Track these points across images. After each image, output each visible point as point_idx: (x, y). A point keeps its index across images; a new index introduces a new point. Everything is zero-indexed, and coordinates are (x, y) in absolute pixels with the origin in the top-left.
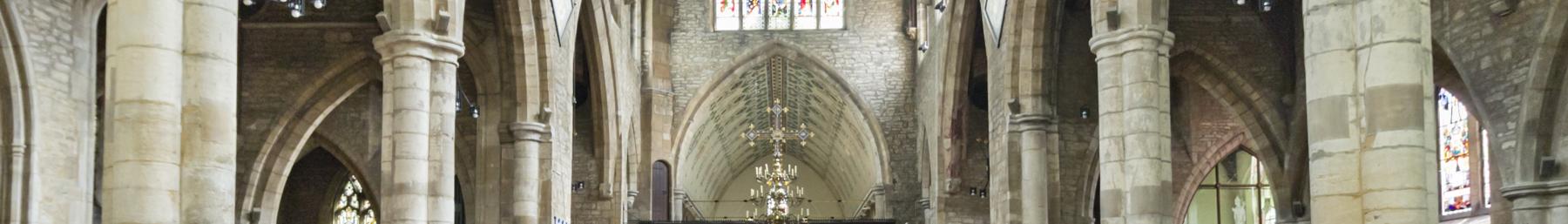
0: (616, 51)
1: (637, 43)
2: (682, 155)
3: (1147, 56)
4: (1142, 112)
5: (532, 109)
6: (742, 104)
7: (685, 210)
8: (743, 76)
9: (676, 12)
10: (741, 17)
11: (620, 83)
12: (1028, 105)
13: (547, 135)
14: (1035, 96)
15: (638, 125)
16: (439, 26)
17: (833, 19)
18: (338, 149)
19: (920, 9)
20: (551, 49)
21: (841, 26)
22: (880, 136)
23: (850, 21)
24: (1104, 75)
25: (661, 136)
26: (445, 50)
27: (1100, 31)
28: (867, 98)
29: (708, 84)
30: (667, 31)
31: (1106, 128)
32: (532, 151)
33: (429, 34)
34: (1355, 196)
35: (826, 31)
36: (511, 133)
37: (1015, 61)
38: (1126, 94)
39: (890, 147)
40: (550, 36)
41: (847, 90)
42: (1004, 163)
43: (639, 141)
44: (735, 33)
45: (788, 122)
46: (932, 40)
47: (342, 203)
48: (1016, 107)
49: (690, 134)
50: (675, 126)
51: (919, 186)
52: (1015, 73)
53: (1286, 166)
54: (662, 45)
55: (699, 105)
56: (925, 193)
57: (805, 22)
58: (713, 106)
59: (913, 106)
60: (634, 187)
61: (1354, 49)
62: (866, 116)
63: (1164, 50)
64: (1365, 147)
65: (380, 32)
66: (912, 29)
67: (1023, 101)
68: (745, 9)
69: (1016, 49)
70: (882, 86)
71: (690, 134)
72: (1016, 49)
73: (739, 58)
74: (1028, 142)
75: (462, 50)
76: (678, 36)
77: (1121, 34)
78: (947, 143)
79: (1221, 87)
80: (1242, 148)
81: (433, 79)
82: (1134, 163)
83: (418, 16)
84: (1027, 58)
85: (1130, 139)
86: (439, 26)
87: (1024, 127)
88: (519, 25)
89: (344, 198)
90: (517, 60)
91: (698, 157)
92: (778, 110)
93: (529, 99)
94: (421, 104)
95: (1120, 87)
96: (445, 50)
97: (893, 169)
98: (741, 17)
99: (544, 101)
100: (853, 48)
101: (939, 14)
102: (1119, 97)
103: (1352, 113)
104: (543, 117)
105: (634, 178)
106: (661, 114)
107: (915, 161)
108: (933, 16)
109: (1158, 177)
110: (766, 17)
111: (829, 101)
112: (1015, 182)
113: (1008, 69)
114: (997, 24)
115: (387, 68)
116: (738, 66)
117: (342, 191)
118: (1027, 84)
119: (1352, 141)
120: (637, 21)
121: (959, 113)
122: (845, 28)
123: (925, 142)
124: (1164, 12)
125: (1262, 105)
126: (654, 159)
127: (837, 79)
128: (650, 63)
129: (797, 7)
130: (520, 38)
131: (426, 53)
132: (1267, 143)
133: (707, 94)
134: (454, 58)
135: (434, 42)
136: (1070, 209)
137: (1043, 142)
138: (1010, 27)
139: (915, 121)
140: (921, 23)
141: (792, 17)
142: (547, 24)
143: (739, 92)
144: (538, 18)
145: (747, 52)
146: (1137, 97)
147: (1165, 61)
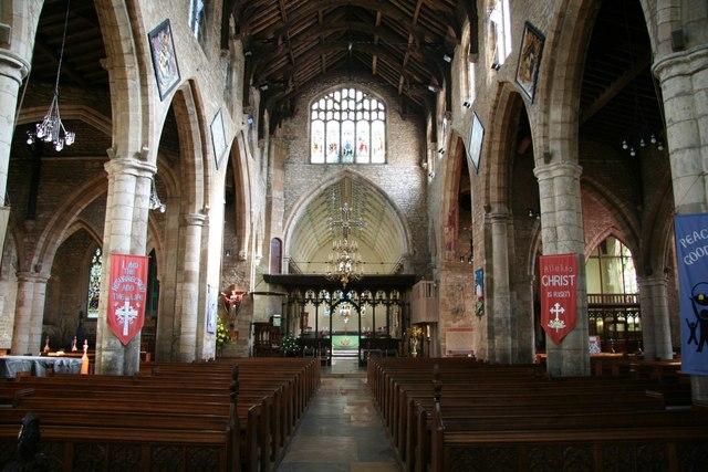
0: (251, 174)
4: (567, 213)
5: (199, 206)
14: (500, 202)
16: (142, 156)
17: (379, 157)
19: (429, 153)
20: (212, 171)
22: (406, 225)
23: (389, 159)
24: (542, 190)
25: (277, 224)
26: (144, 170)
28: (398, 203)
31: (545, 221)
32: (197, 231)
36: (185, 220)
37: (487, 182)
42: (482, 243)
46: (437, 171)
48: (488, 209)
49: (294, 223)
50: (285, 218)
52: (487, 189)
53: (641, 245)
57: (362, 158)
58: (308, 206)
62: (398, 213)
67: (492, 206)
68: (328, 151)
69: (488, 175)
70: (408, 196)
74: (495, 230)
75: (155, 170)
80: (611, 235)
84: (494, 179)
85: (560, 229)
86: (142, 156)
87: (492, 221)
88: (193, 157)
90: (191, 177)
93: (197, 201)
94: (129, 203)
95: (553, 198)
96: (144, 170)
101: (441, 155)
102: (553, 203)
104: (205, 211)
105: (260, 249)
106: (278, 210)
107: (427, 240)
110: (340, 156)
113: (483, 186)
114: (476, 161)
118: (494, 196)
120: (265, 158)
122: (386, 163)
123: (433, 229)
125: (625, 211)
126: (272, 238)
130: (194, 165)
131: (134, 172)
132: (629, 232)
134: (150, 175)
135: (139, 166)
136: (521, 270)
137: (502, 228)
139: (427, 216)
140: (430, 161)
141: (355, 156)
142: (210, 157)
143: (323, 198)
145: (329, 176)
146: (563, 203)
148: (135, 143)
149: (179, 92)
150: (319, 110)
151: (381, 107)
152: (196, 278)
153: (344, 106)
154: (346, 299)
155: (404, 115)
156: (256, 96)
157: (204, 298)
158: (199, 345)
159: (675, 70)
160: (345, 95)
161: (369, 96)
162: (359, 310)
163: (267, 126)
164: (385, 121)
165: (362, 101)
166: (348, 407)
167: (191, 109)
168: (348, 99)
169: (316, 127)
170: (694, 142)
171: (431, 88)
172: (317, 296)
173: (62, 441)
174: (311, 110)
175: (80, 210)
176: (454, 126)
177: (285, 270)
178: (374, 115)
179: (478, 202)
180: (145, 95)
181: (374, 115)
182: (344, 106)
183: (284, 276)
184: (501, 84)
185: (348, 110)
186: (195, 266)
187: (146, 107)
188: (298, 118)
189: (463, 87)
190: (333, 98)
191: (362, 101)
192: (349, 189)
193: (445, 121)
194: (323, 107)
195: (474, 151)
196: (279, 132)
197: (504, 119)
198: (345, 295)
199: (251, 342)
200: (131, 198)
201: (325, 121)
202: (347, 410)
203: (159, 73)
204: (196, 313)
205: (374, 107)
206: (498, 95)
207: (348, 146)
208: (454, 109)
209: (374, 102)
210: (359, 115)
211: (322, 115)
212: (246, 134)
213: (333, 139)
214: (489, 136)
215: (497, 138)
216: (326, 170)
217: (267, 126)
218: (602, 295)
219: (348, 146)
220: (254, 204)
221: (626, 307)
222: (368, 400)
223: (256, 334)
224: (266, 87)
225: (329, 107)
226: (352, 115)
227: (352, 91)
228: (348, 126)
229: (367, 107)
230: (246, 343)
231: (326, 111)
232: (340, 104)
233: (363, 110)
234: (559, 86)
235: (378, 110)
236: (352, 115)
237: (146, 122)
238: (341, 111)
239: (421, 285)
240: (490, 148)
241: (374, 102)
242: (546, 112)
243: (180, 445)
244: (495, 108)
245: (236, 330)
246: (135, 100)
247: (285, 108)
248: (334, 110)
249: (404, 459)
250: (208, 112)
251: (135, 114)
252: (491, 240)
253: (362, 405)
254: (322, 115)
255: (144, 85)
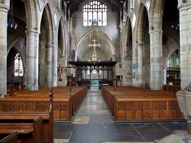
0: (65, 30)
1: (69, 28)
2: (77, 49)
3: (158, 35)
5: (51, 42)
6: (88, 39)
7: (77, 59)
8: (88, 34)
9: (76, 23)
10: (88, 23)
11: (66, 36)
12: (139, 42)
13: (53, 46)
15: (69, 43)
16: (36, 29)
17: (105, 24)
18: (16, 49)
19: (121, 22)
20: (54, 31)
21: (106, 25)
24: (151, 38)
25: (73, 45)
27: (150, 31)
28: (111, 39)
29: (81, 36)
30: (74, 26)
31: (151, 47)
33: (34, 30)
34: (187, 61)
35: (104, 26)
36: (47, 46)
38: (155, 42)
39: (115, 48)
40: (54, 29)
41: (107, 37)
43: (69, 46)
44: (87, 26)
45: (97, 43)
46: (123, 29)
47: (16, 58)
48: (137, 42)
49: (78, 45)
50: (76, 43)
51: (121, 55)
52: (137, 36)
54: (73, 29)
55: (80, 40)
56: (122, 56)
57: (100, 24)
59: (120, 40)
60: (68, 55)
61: (187, 37)
62: (111, 42)
63: (161, 34)
64: (188, 53)
65: (26, 30)
66: (119, 26)
67: (138, 41)
68: (89, 21)
69: (137, 31)
70: (114, 36)
71: (78, 45)
72: (137, 31)
73: (87, 31)
74: (139, 48)
75: (40, 33)
76: (76, 27)
77: (154, 31)
78: (126, 47)
79: (173, 39)
81: (35, 38)
82: (156, 53)
83: (32, 27)
85: (155, 49)
87: (138, 46)
88: (49, 27)
89: (16, 57)
90: (48, 33)
91: (80, 49)
92: (95, 45)
93: (50, 40)
97: (116, 52)
98: (88, 23)
99: (53, 40)
100: (108, 29)
101: (124, 24)
103: (187, 48)
104: (53, 43)
105: (68, 53)
106: (73, 41)
108: (123, 24)
109: (160, 56)
110: (93, 24)
111: (104, 39)
112: (137, 55)
113: (136, 35)
114: (134, 27)
115: (27, 36)
116: (88, 32)
117: (16, 56)
118: (139, 38)
119: (186, 52)
120: (69, 24)
121: (128, 42)
122: (107, 26)
124: (161, 27)
126: (72, 50)
127: (106, 35)
128: (71, 32)
129: (98, 22)
130: (49, 29)
131: (34, 33)
133: (82, 38)
134: (38, 34)
135: (35, 32)
137: (142, 48)
138: (136, 28)
140: (121, 25)
141: (97, 24)
142: (54, 27)
143: (87, 37)
144: (52, 26)
145: (89, 30)
147: (161, 36)
148: (33, 25)
149: (45, 8)
150: (86, 8)
151: (106, 7)
152: (51, 63)
153: (94, 7)
154: (95, 68)
155: (113, 10)
156: (65, 4)
157: (53, 69)
158: (52, 83)
159: (183, 8)
160: (94, 3)
161: (102, 4)
162: (98, 72)
163: (69, 14)
164: (107, 12)
165: (99, 5)
166: (96, 99)
167: (48, 15)
168: (95, 4)
169: (85, 14)
170: (186, 28)
171: (121, 2)
172: (86, 68)
173: (33, 102)
174: (83, 9)
175: (14, 43)
176: (128, 15)
177: (76, 60)
178: (103, 10)
179: (134, 40)
180: (36, 10)
181: (103, 10)
182: (94, 7)
183: (76, 62)
184: (142, 4)
185: (95, 8)
186: (50, 60)
187: (36, 14)
188: (78, 11)
189: (131, 3)
190: (90, 4)
191: (99, 5)
192: (95, 33)
193: (125, 13)
194: (87, 7)
195: (133, 24)
196: (73, 15)
197: (142, 14)
198: (95, 68)
199: (66, 82)
200: (34, 41)
201: (88, 12)
202: (95, 100)
203: (39, 3)
204: (51, 73)
205: (103, 7)
206: (141, 7)
207: (95, 20)
208: (128, 9)
209: (103, 5)
210: (99, 10)
211: (87, 10)
212: (63, 18)
213: (90, 18)
214: (138, 19)
215: (140, 20)
216: (88, 28)
217: (69, 14)
218: (174, 68)
219: (95, 20)
220: (66, 40)
221: (101, 69)
222: (101, 98)
223: (68, 80)
224: (69, 2)
225: (89, 7)
226: (96, 10)
227: (96, 2)
228: (95, 13)
229: (101, 7)
230: (65, 82)
231: (88, 9)
232: (92, 6)
233: (100, 8)
234: (157, 7)
235: (104, 8)
236: (96, 10)
237: (37, 19)
238: (93, 9)
239: (117, 65)
240: (138, 23)
241: (103, 5)
242: (153, 15)
243: (59, 102)
244: (140, 11)
245: (61, 78)
246: (33, 12)
247: (75, 8)
248: (90, 8)
249: (111, 112)
250: (52, 13)
251: (33, 16)
252: (138, 52)
253: (99, 99)
254: (87, 10)
255: (35, 7)
